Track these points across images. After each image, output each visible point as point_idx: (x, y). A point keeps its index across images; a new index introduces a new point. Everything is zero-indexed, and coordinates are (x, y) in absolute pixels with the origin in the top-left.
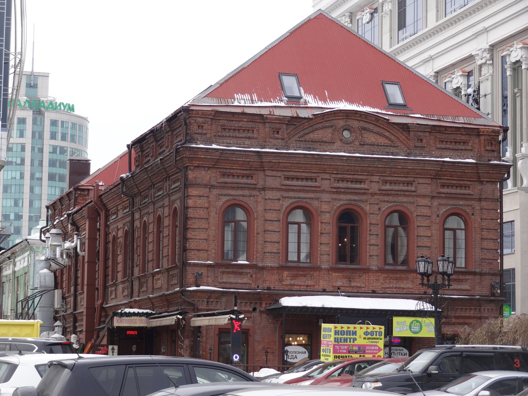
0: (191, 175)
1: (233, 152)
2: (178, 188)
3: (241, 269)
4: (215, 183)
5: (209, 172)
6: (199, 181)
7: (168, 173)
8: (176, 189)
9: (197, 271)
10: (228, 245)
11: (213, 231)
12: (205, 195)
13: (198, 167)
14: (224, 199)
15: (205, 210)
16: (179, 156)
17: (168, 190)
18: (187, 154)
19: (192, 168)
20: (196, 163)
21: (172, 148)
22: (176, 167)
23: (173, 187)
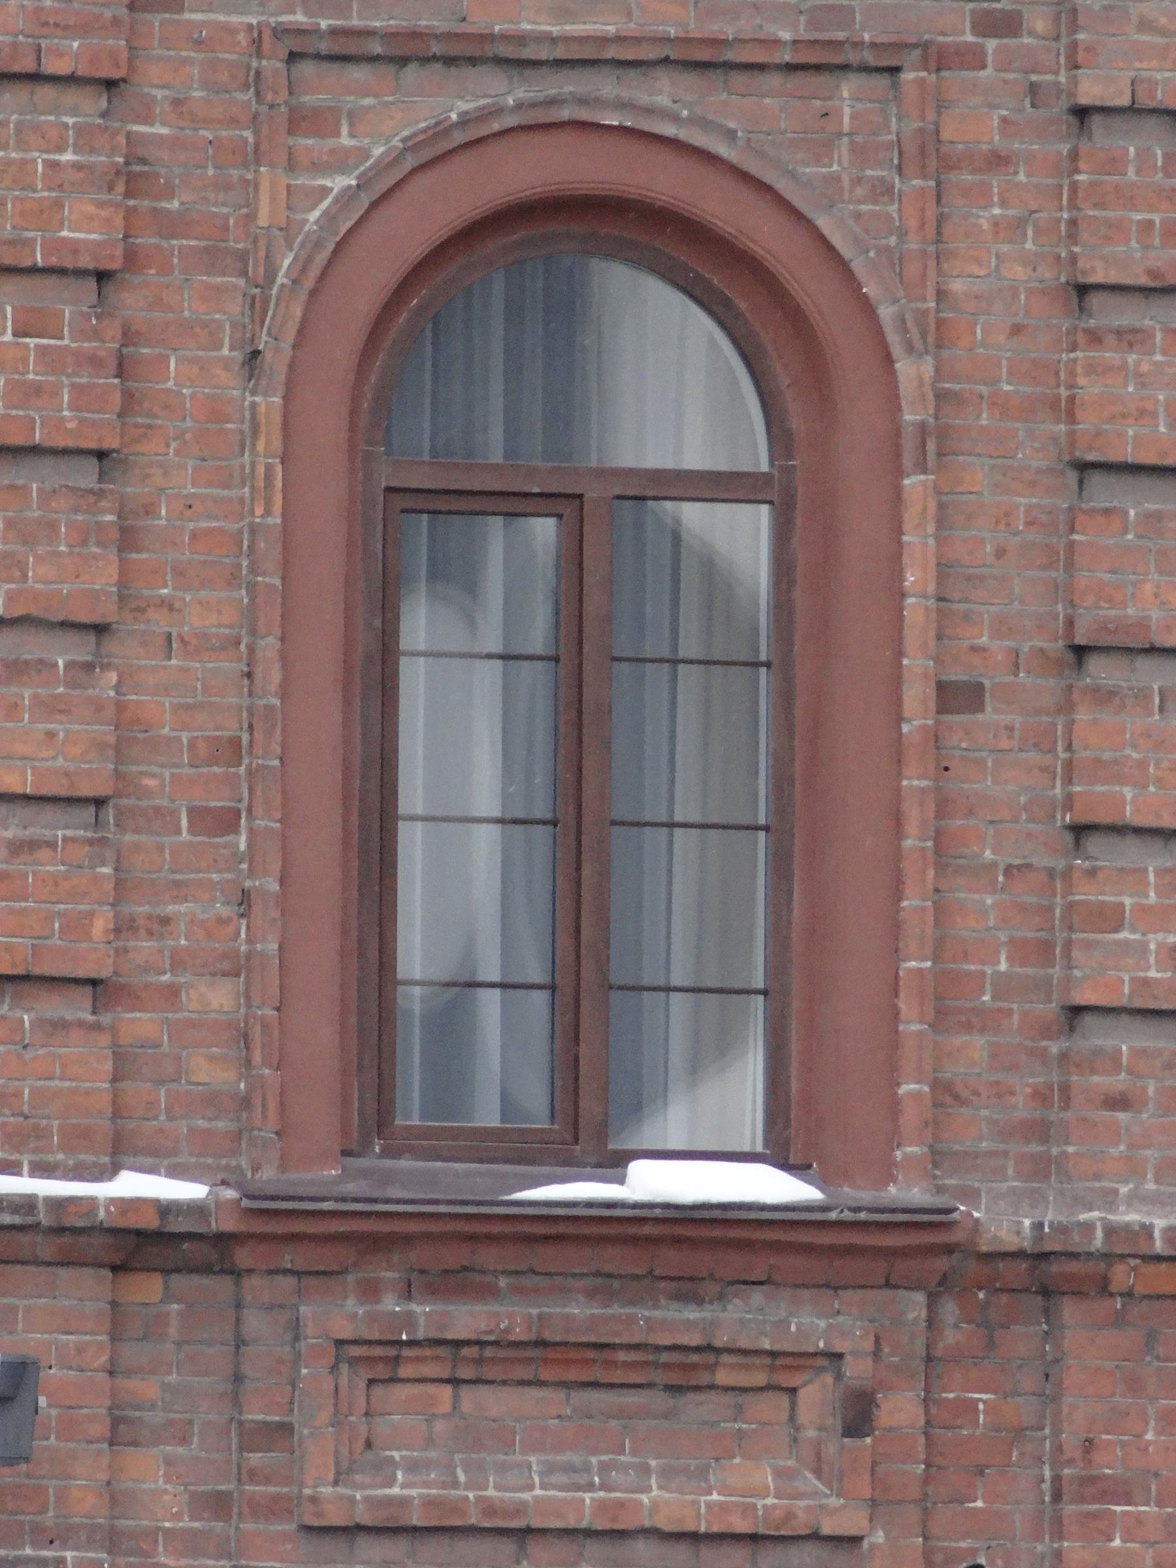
3: (687, 1288)
10: (462, 893)
11: (205, 661)
12: (68, 53)
14: (386, 118)
15: (70, 305)
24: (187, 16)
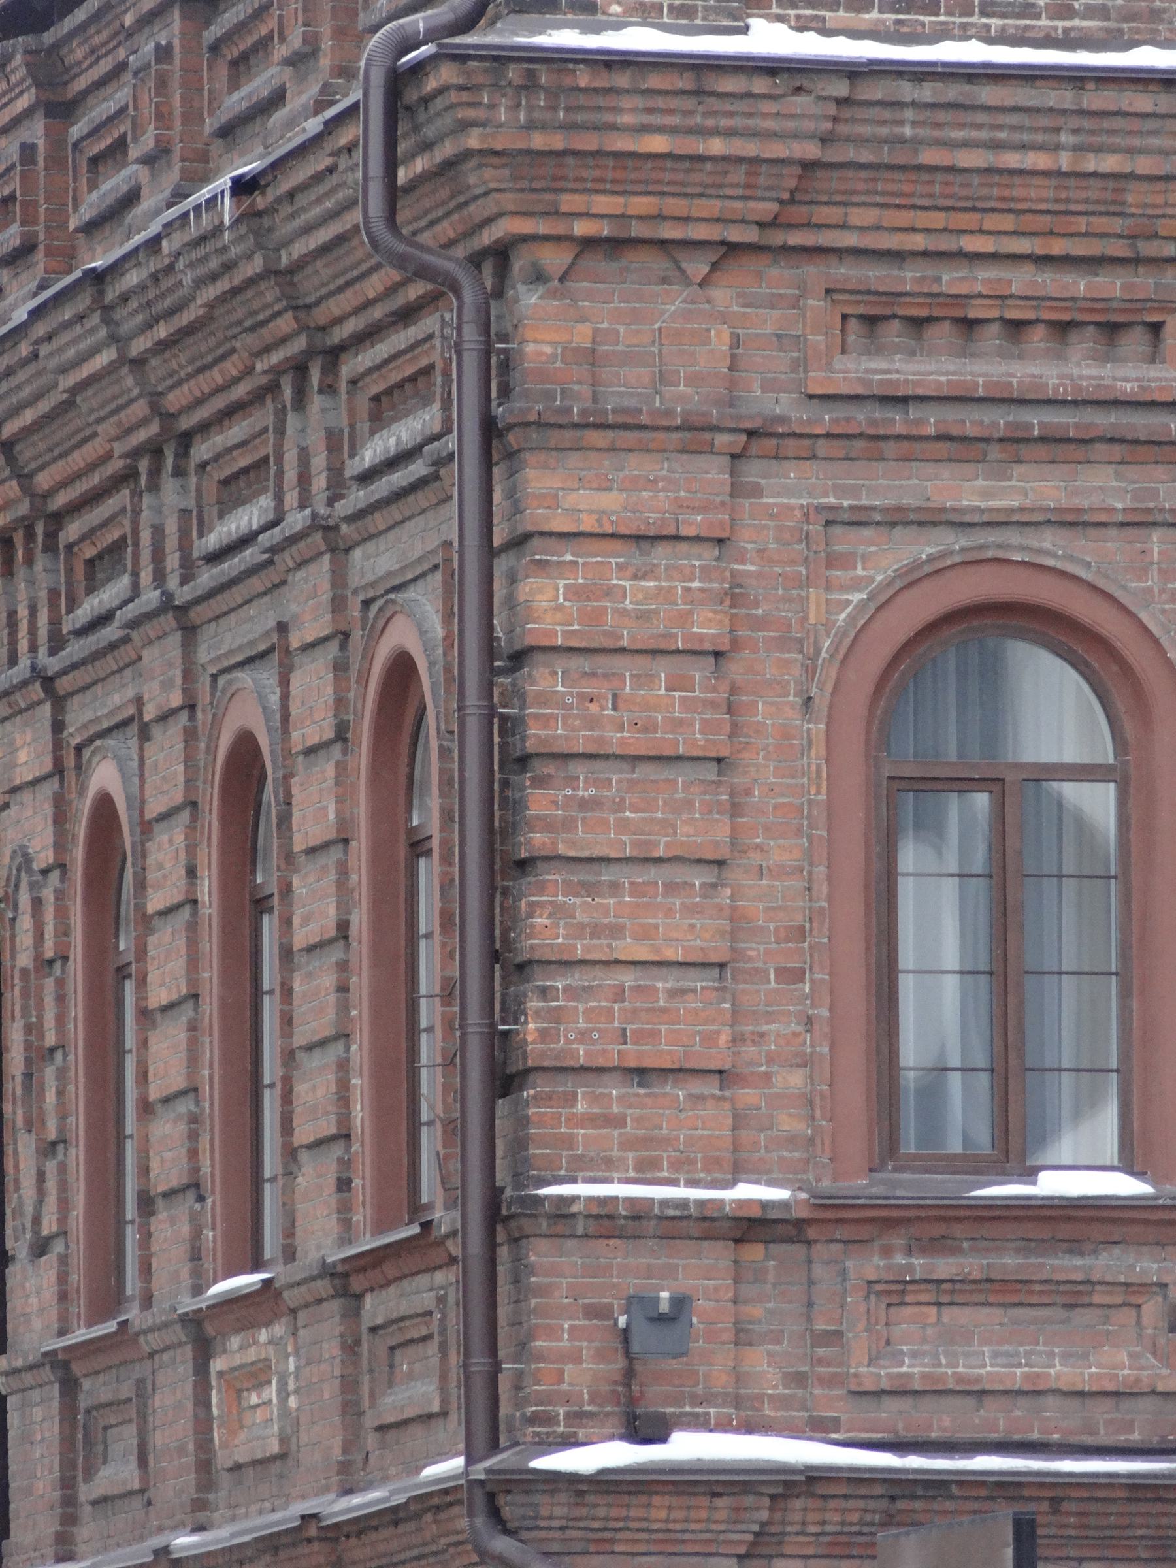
0: (547, 329)
1: (953, 92)
2: (418, 469)
3: (1074, 1246)
4: (784, 406)
5: (722, 295)
6: (625, 387)
7: (320, 316)
8: (399, 478)
9: (634, 1284)
10: (937, 1015)
11: (784, 881)
12: (694, 524)
13: (615, 245)
14: (883, 559)
15: (700, 671)
16: (427, 146)
17: (320, 482)
18: (504, 122)
19: (555, 259)
20: (596, 210)
21: (345, 72)
22: (400, 262)
23: (371, 453)
24: (765, 500)
